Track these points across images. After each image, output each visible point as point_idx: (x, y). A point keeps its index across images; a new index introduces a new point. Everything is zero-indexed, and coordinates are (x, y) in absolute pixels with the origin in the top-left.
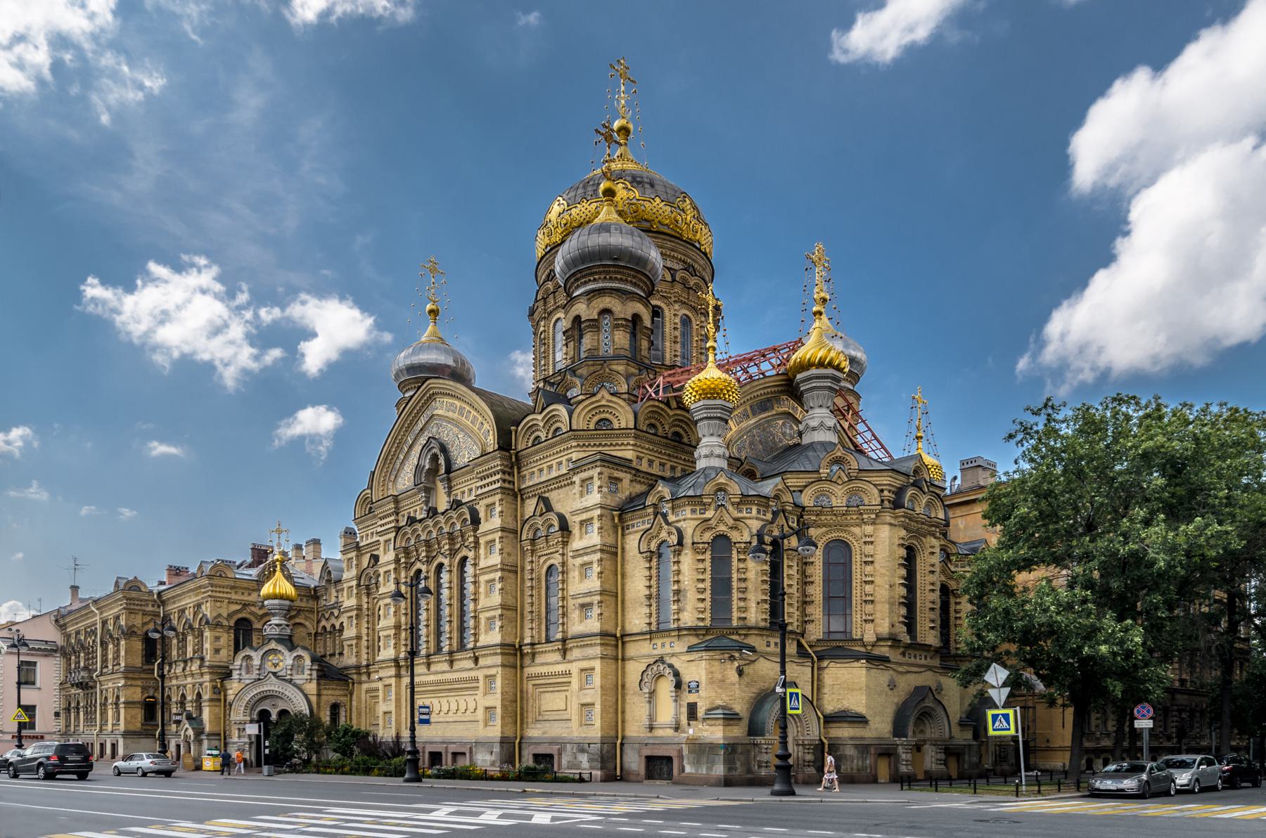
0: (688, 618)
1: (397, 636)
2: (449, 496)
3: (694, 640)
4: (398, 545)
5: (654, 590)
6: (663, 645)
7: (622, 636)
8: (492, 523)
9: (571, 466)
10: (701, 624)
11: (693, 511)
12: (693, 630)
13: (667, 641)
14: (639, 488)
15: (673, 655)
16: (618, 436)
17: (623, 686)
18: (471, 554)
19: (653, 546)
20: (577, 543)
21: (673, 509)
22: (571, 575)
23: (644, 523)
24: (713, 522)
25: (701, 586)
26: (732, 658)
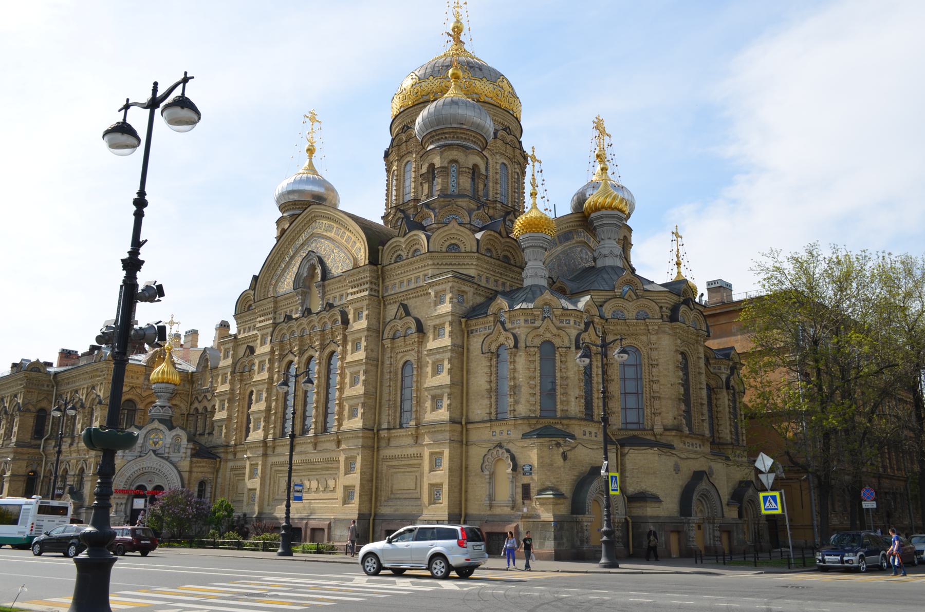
5: (494, 385)
6: (501, 433)
14: (480, 300)
16: (464, 258)
17: (466, 468)
20: (432, 344)
23: (485, 328)
24: (541, 330)
26: (558, 445)
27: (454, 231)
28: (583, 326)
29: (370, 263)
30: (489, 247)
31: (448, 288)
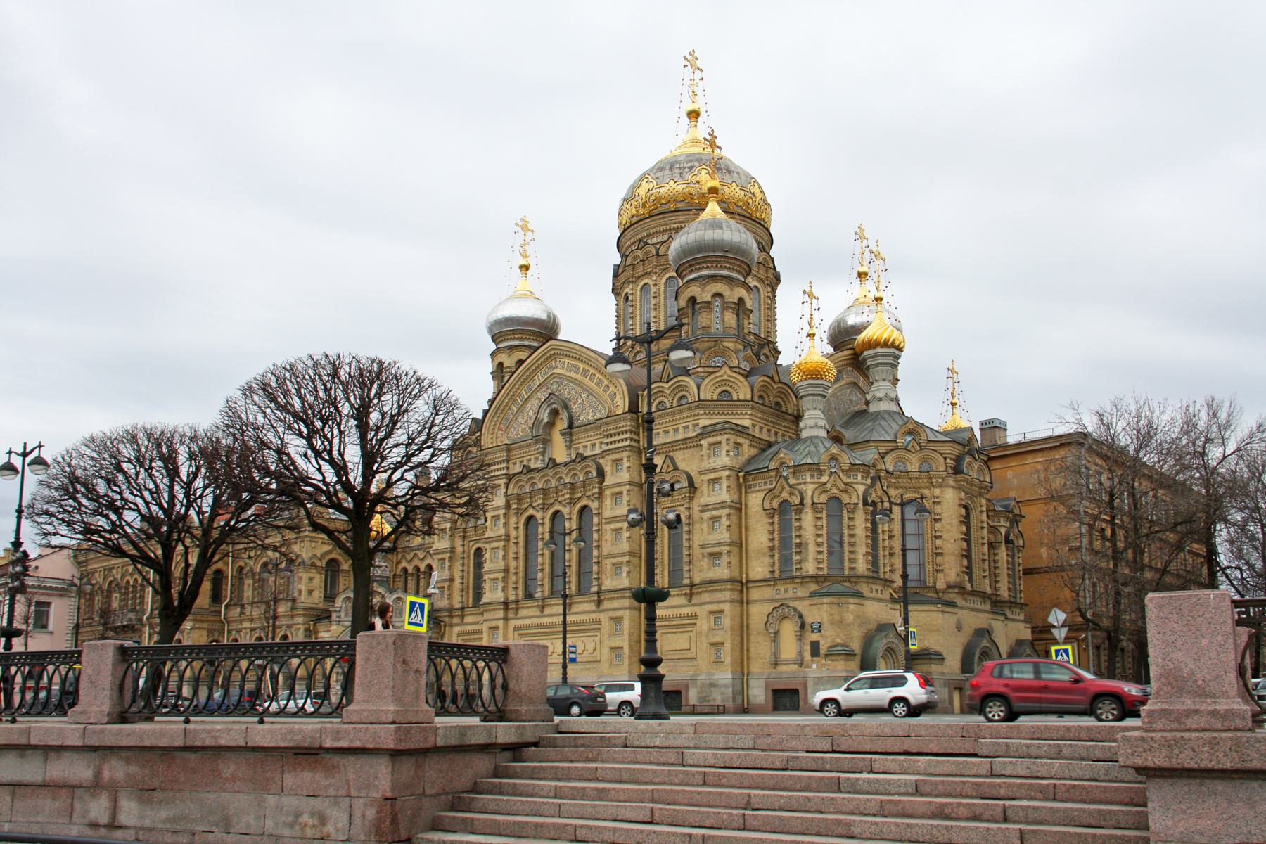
0: (810, 568)
1: (505, 579)
2: (569, 447)
3: (813, 587)
5: (776, 542)
6: (786, 591)
7: (747, 582)
9: (698, 431)
11: (812, 476)
12: (815, 578)
14: (754, 451)
15: (797, 599)
16: (738, 407)
18: (594, 505)
19: (775, 504)
22: (697, 526)
24: (828, 486)
28: (869, 481)
29: (630, 411)
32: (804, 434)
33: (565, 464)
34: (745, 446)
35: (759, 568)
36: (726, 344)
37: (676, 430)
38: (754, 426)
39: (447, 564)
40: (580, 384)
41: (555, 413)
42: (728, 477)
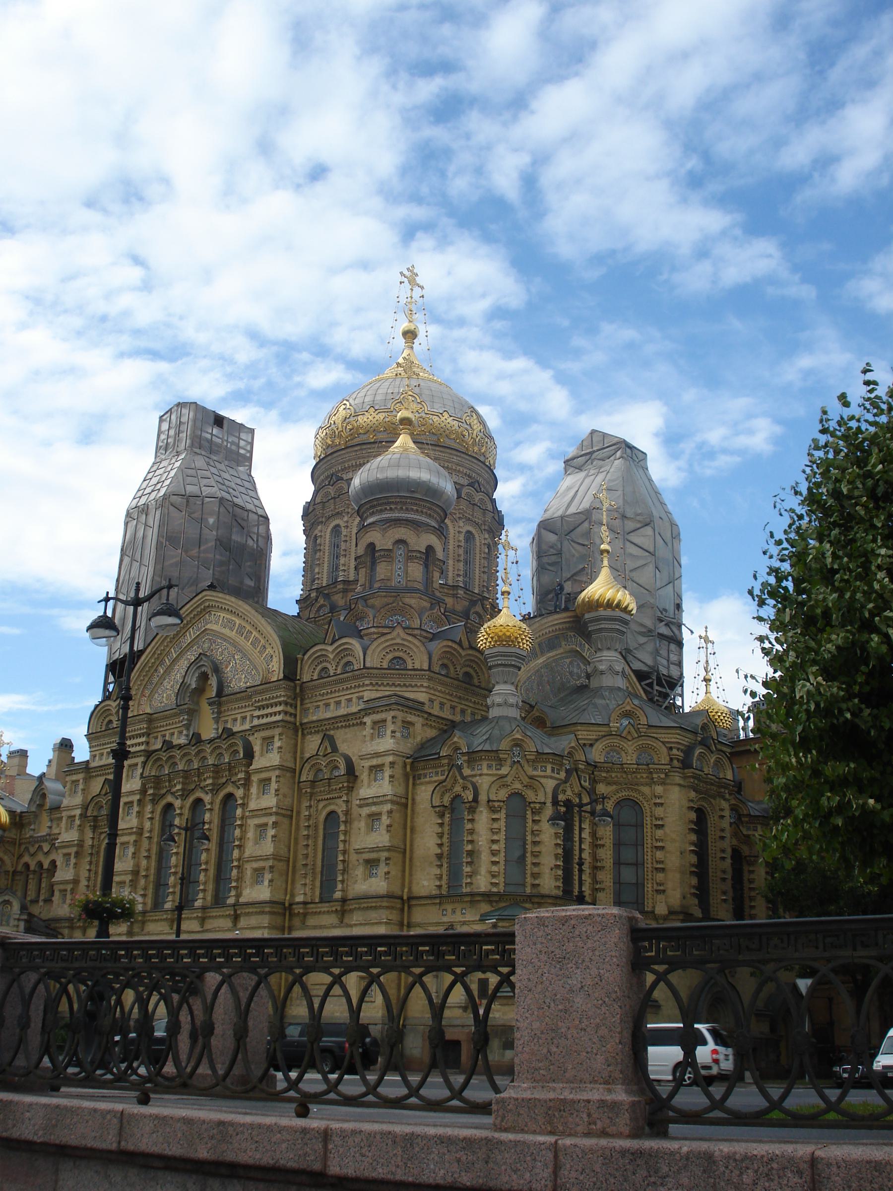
0: (482, 883)
2: (217, 722)
3: (485, 908)
4: (146, 774)
5: (446, 849)
6: (454, 912)
7: (409, 898)
8: (268, 759)
9: (362, 706)
10: (495, 890)
11: (489, 767)
12: (487, 896)
13: (458, 906)
14: (431, 733)
18: (239, 793)
19: (447, 800)
20: (366, 791)
21: (469, 762)
22: (355, 824)
23: (437, 773)
24: (509, 779)
25: (495, 847)
27: (398, 641)
28: (563, 775)
29: (286, 678)
30: (446, 661)
31: (389, 719)
32: (493, 713)
33: (211, 741)
34: (418, 726)
35: (426, 881)
36: (407, 600)
37: (338, 703)
38: (431, 701)
39: (73, 861)
40: (234, 644)
41: (204, 677)
42: (392, 764)
